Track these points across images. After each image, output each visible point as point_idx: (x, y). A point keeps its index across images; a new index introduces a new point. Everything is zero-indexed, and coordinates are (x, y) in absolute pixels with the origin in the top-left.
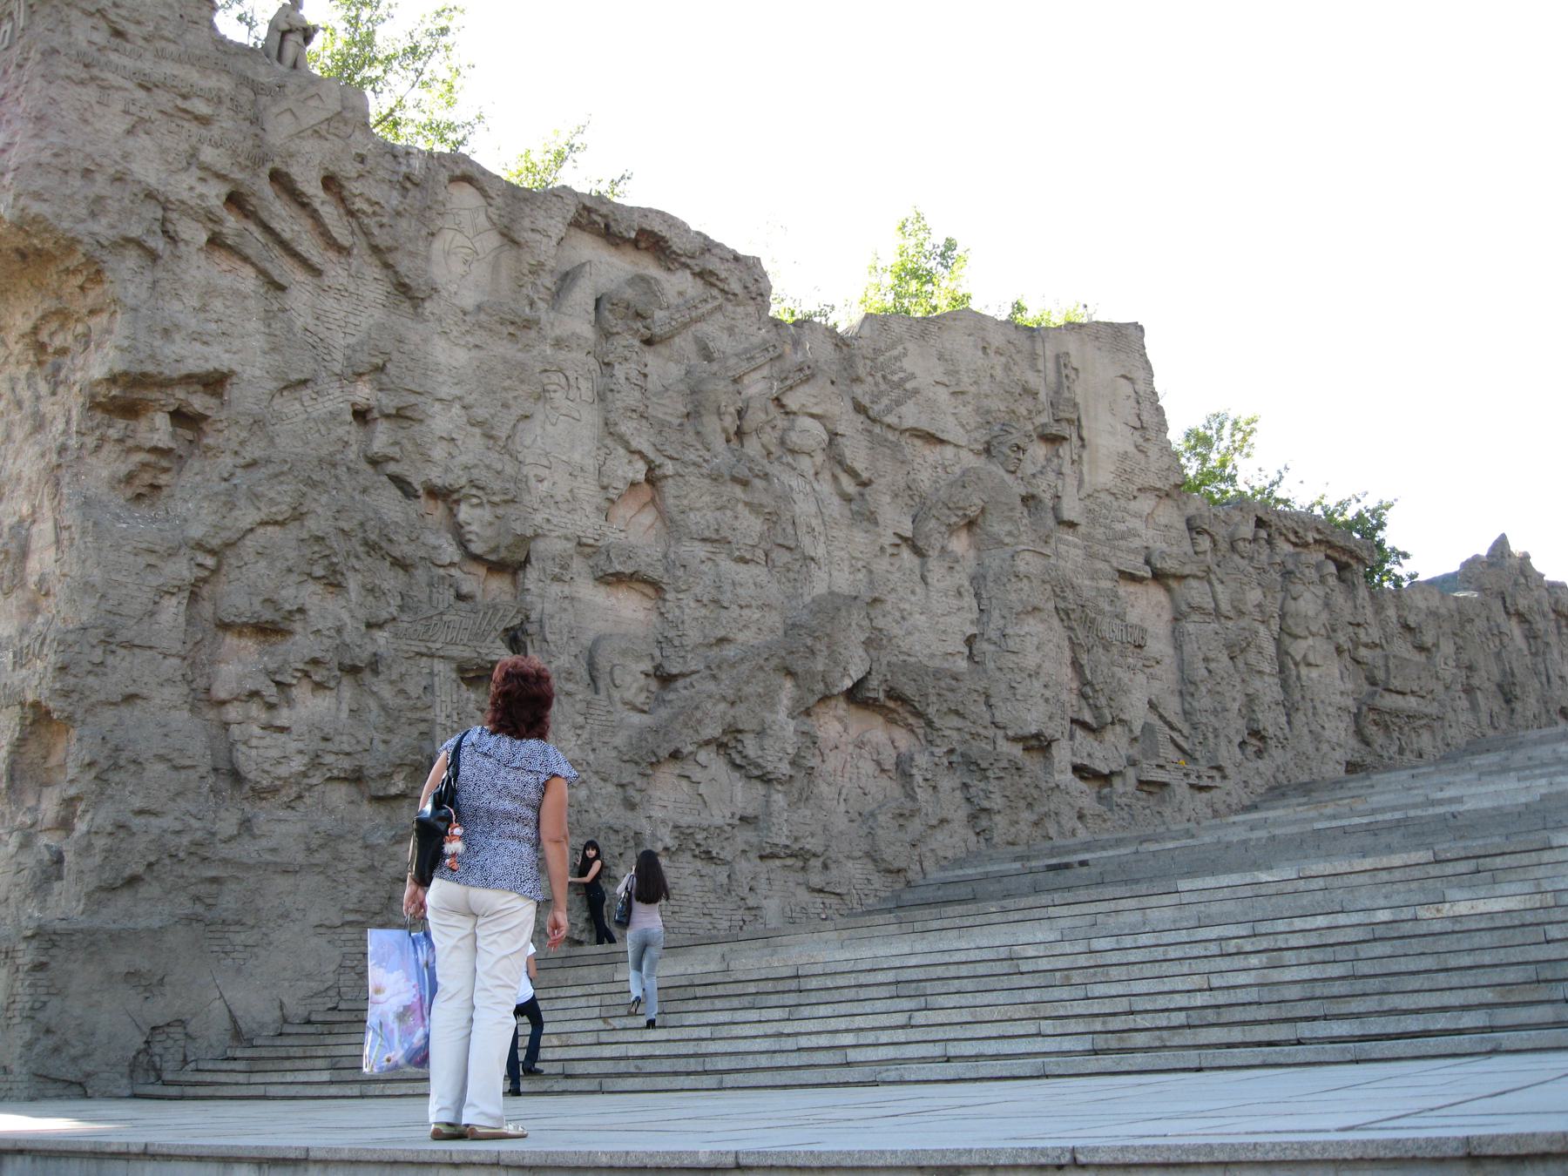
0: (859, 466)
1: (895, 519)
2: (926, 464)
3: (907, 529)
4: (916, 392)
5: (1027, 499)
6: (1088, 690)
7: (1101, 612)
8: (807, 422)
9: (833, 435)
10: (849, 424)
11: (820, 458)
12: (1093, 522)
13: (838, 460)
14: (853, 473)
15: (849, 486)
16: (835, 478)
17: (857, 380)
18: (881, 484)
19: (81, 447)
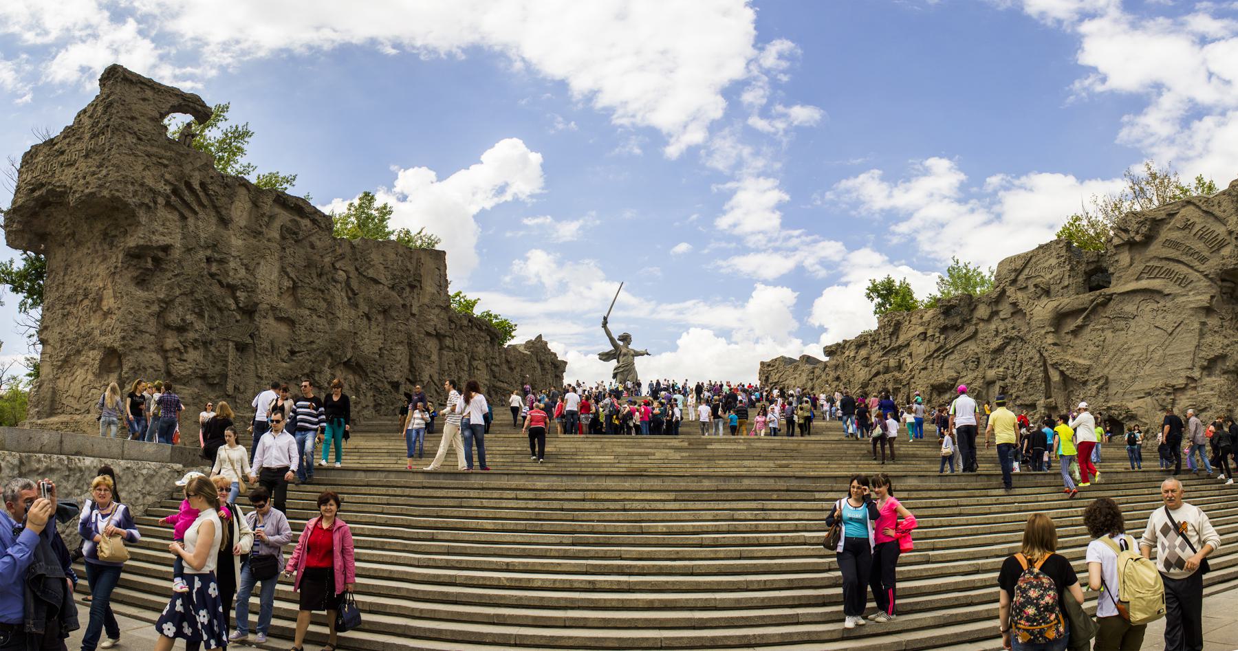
0: (355, 288)
1: (364, 308)
2: (373, 292)
3: (366, 310)
4: (374, 265)
5: (404, 306)
6: (413, 369)
7: (419, 344)
8: (341, 272)
9: (348, 277)
10: (353, 274)
11: (343, 285)
12: (420, 315)
13: (348, 284)
14: (352, 290)
15: (350, 295)
16: (347, 291)
17: (357, 260)
18: (361, 295)
19: (123, 267)
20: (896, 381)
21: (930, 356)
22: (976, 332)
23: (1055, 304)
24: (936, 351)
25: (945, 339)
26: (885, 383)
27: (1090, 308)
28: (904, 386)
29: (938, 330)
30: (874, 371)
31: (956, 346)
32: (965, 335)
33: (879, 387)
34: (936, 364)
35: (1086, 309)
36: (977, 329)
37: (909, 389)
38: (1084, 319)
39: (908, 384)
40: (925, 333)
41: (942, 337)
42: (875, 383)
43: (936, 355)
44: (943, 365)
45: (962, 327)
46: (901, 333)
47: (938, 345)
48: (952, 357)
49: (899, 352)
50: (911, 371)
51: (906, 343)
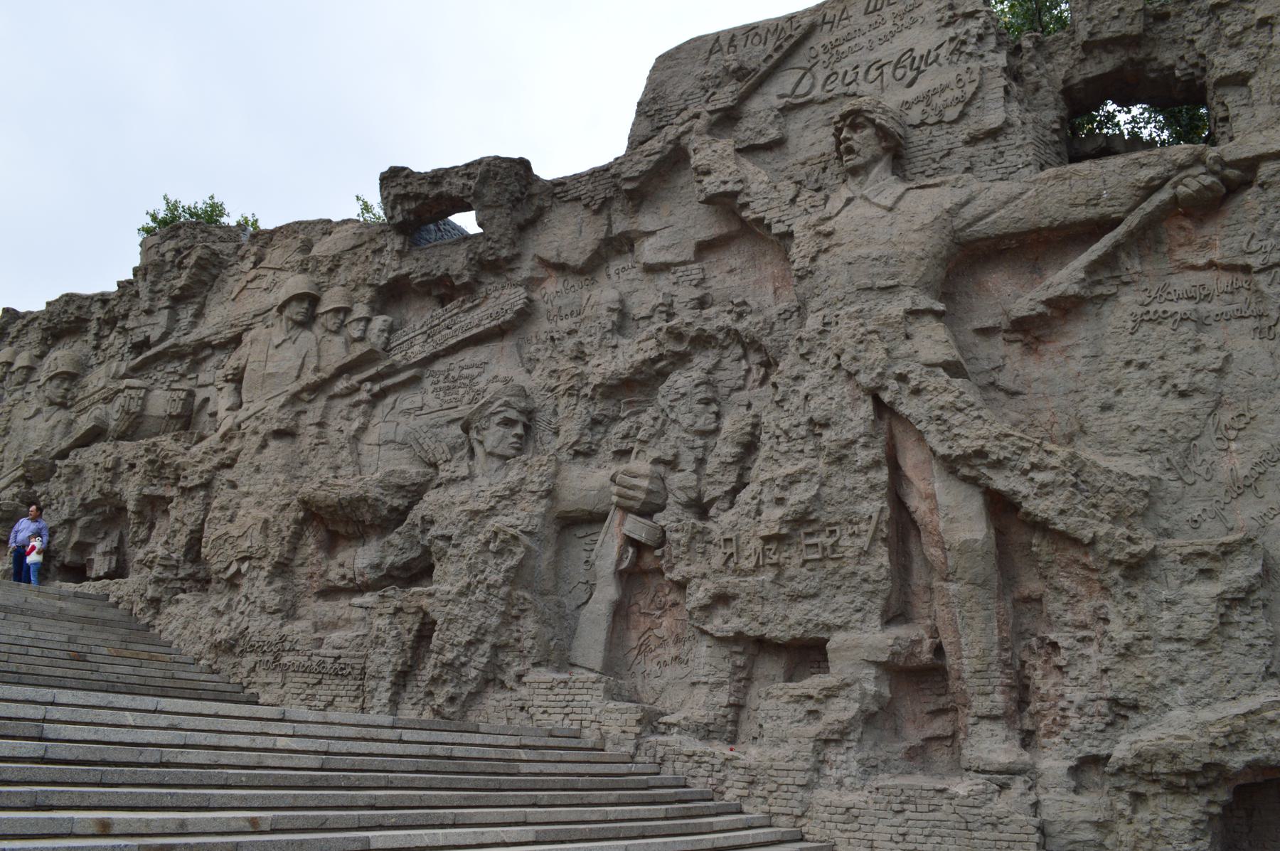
20: (159, 468)
21: (316, 389)
22: (526, 314)
23: (945, 197)
24: (345, 370)
25: (391, 330)
26: (114, 471)
27: (1133, 220)
28: (186, 491)
29: (368, 293)
30: (84, 423)
31: (434, 357)
32: (480, 318)
33: (90, 487)
34: (335, 423)
35: (1104, 225)
36: (530, 301)
37: (207, 508)
38: (1092, 268)
39: (207, 485)
40: (312, 300)
41: (379, 322)
42: (78, 471)
43: (341, 385)
44: (363, 429)
45: (470, 289)
46: (214, 299)
47: (359, 349)
48: (410, 399)
49: (196, 365)
50: (227, 437)
51: (229, 333)
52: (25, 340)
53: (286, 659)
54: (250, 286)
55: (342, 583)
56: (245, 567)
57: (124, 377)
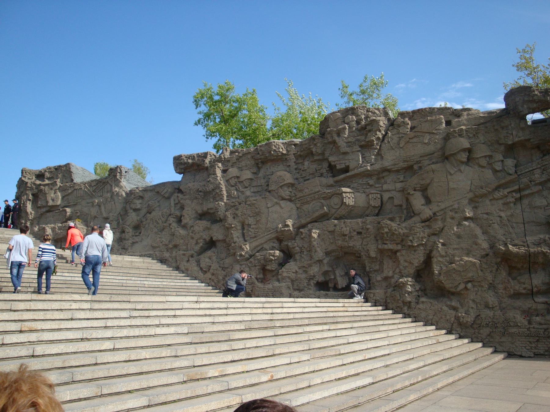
43: (497, 195)
52: (243, 164)
53: (513, 330)
54: (411, 141)
55: (524, 291)
56: (469, 285)
57: (331, 186)
